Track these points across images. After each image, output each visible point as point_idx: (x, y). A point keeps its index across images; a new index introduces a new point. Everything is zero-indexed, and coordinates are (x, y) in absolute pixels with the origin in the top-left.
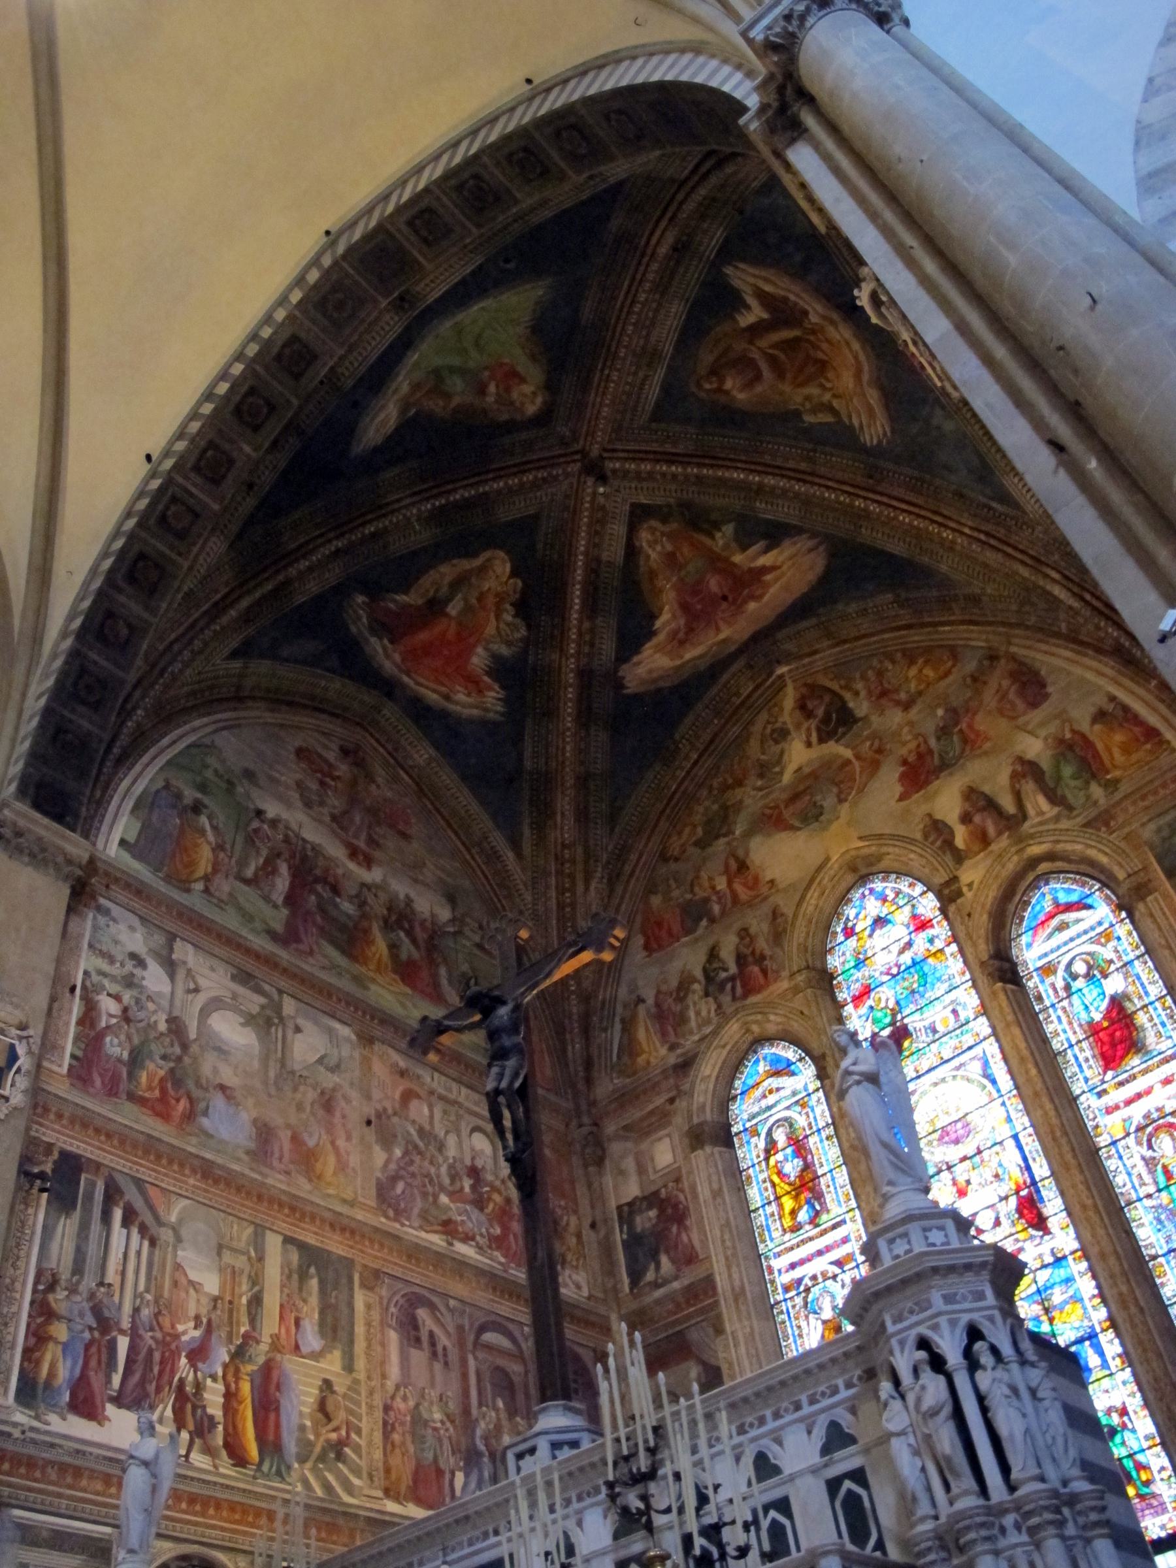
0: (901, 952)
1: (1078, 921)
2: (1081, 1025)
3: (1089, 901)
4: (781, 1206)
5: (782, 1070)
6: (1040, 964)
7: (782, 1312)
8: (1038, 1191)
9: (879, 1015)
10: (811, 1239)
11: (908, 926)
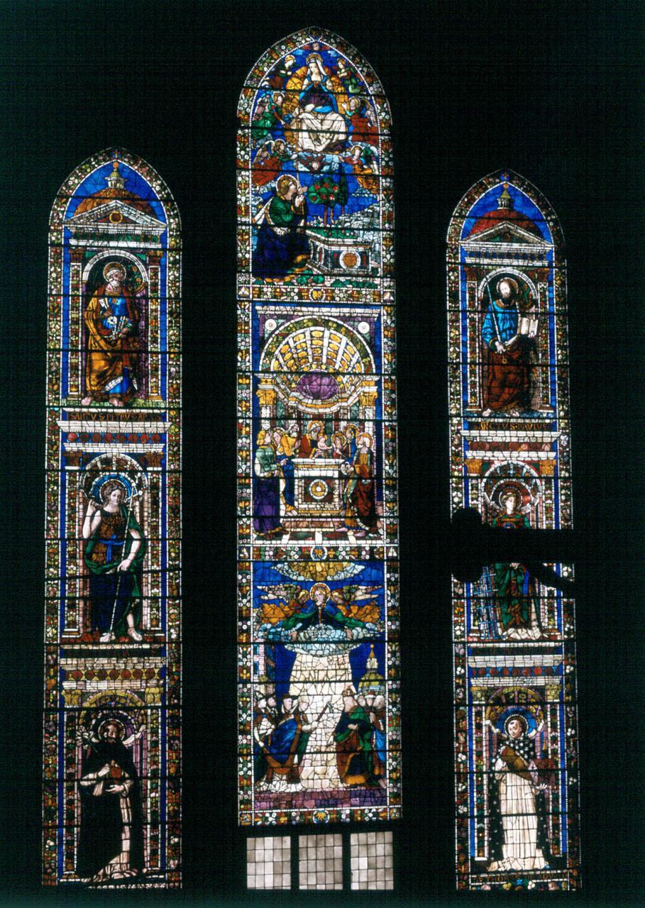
0: (329, 149)
1: (521, 240)
2: (481, 348)
3: (541, 227)
4: (89, 362)
5: (137, 196)
6: (469, 260)
7: (56, 483)
8: (380, 489)
9: (280, 206)
10: (116, 418)
11: (348, 123)
